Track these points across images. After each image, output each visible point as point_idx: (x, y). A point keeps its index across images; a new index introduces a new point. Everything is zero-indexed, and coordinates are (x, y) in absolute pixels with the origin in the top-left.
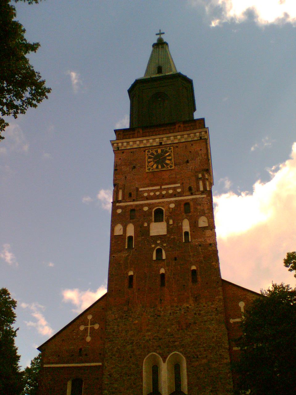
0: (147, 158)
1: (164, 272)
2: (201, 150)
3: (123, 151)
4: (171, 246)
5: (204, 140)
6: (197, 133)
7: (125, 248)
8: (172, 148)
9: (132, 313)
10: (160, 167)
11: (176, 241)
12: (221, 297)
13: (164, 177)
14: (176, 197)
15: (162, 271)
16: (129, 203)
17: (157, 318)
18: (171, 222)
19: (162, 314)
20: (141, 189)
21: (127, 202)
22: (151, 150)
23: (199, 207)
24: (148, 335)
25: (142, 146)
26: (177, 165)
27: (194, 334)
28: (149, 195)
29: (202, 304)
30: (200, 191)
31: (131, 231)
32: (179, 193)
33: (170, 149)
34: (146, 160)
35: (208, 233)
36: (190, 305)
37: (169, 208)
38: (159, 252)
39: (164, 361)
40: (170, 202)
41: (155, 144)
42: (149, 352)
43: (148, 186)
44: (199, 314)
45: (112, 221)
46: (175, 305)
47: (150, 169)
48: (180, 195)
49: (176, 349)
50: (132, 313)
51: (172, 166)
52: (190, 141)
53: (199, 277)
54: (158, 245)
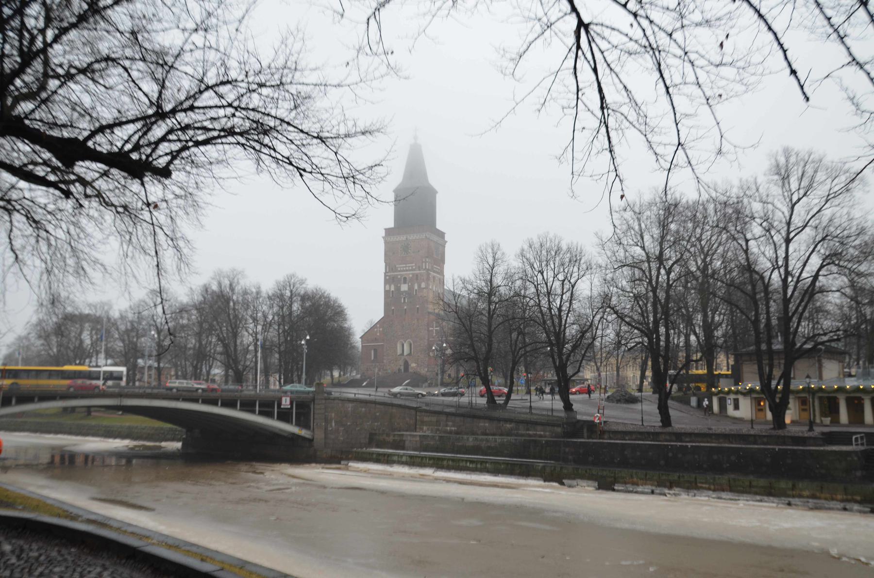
31: (393, 289)
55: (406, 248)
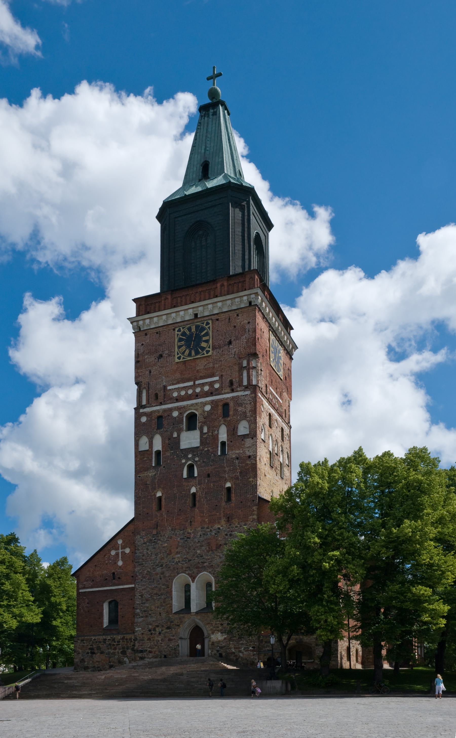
0: (176, 340)
1: (195, 491)
2: (249, 323)
3: (145, 332)
4: (205, 460)
5: (254, 307)
6: (244, 296)
7: (152, 466)
8: (210, 322)
9: (161, 536)
10: (193, 353)
11: (210, 454)
12: (255, 517)
13: (198, 368)
14: (212, 396)
15: (193, 490)
16: (154, 407)
17: (186, 541)
18: (205, 430)
19: (192, 536)
20: (169, 388)
21: (152, 406)
22: (183, 328)
23: (240, 409)
24: (178, 557)
25: (170, 322)
26: (216, 348)
27: (223, 555)
28: (179, 395)
29: (234, 524)
30: (244, 386)
31: (158, 444)
32: (217, 389)
33: (207, 324)
34: (176, 344)
35: (248, 442)
36: (222, 526)
37: (204, 411)
38: (191, 468)
39: (193, 581)
40: (205, 403)
41: (187, 318)
42: (178, 574)
43: (178, 383)
44: (231, 535)
45: (136, 434)
46: (206, 526)
47: (180, 356)
48: (218, 392)
49: (205, 570)
50: (161, 536)
51: (209, 351)
52: (235, 310)
53: (233, 495)
54: (188, 459)
55: (193, 339)
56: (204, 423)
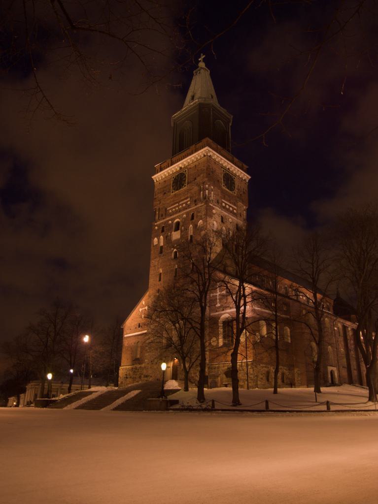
8: (187, 170)
20: (168, 209)
23: (199, 214)
33: (186, 171)
43: (172, 205)
48: (189, 206)
54: (174, 248)
56: (183, 226)
